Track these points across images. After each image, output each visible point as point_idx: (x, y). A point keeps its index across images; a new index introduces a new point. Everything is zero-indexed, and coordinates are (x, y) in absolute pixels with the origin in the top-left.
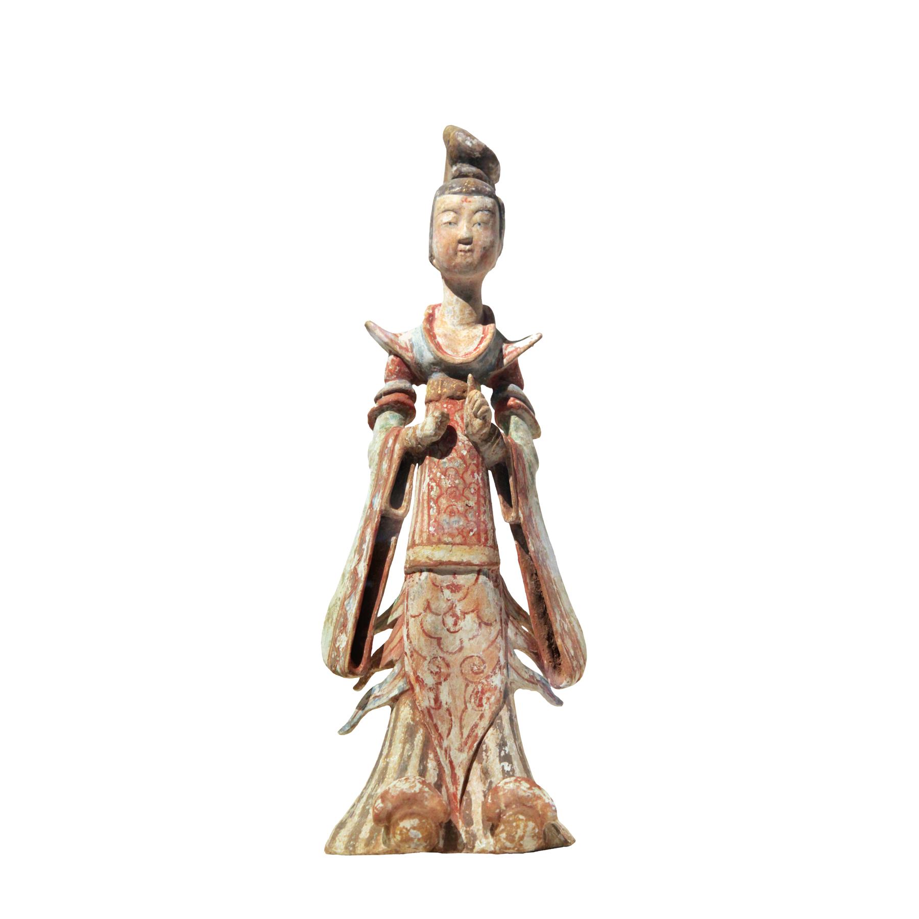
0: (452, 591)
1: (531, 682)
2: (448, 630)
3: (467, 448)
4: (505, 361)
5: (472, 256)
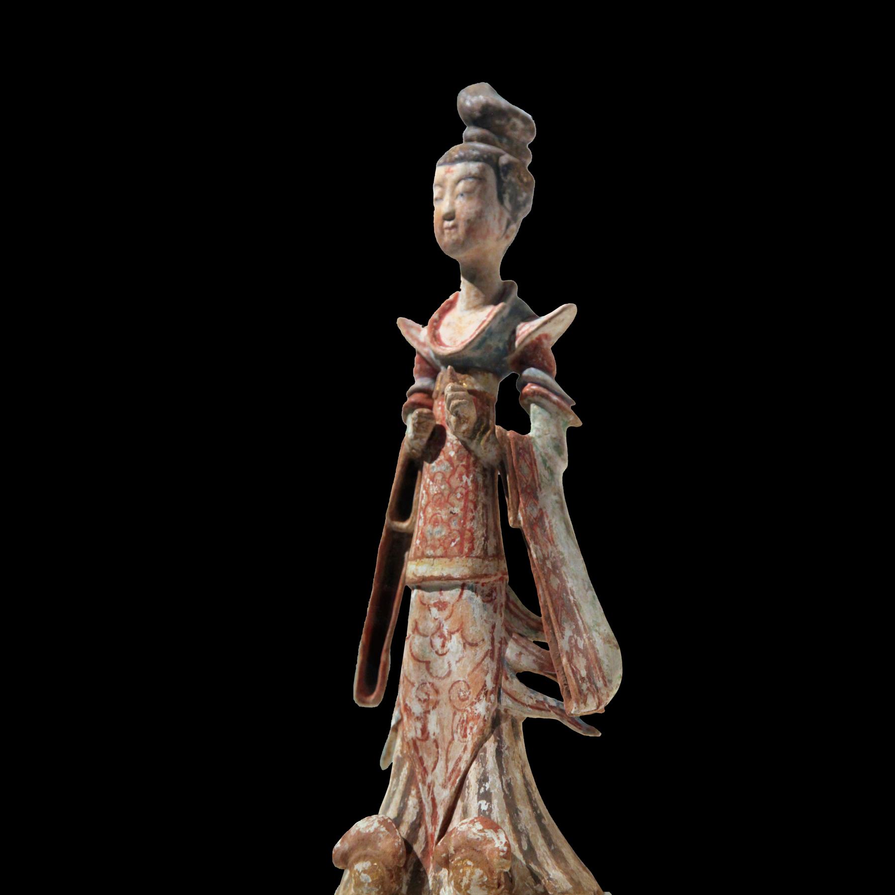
0: (439, 609)
2: (437, 652)
3: (456, 448)
4: (517, 343)
5: (457, 232)
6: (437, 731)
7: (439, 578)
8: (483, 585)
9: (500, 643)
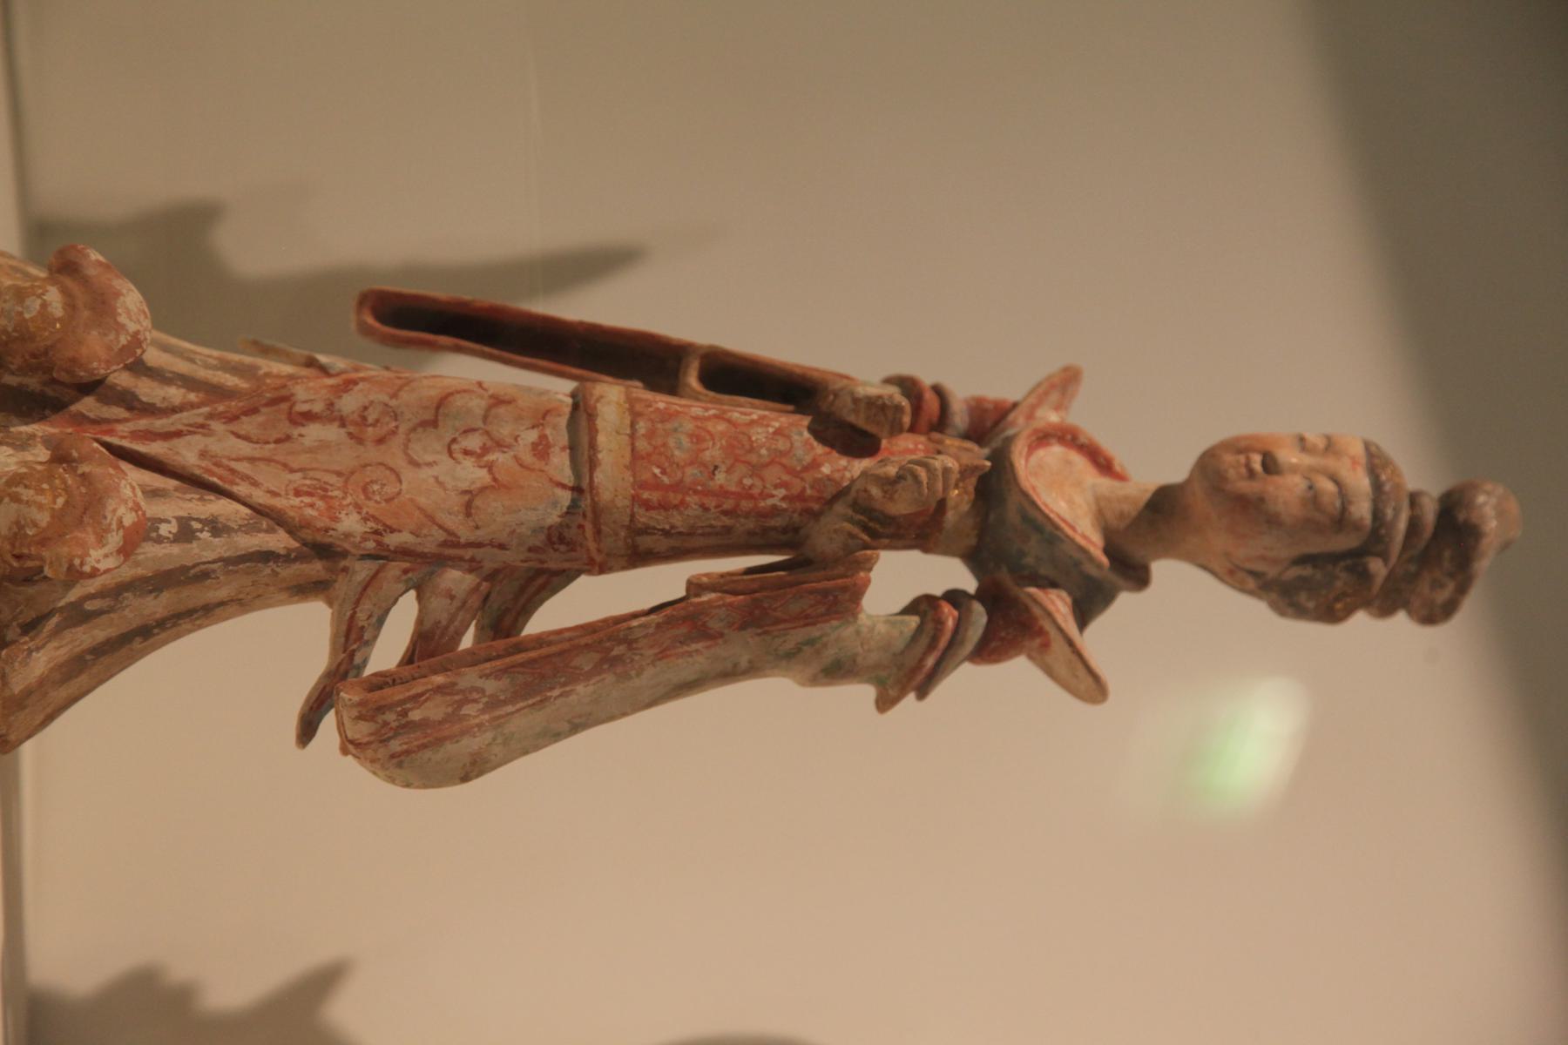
0: (535, 446)
1: (352, 638)
2: (454, 440)
3: (837, 476)
4: (1032, 590)
6: (307, 442)
7: (593, 445)
8: (581, 527)
9: (472, 560)
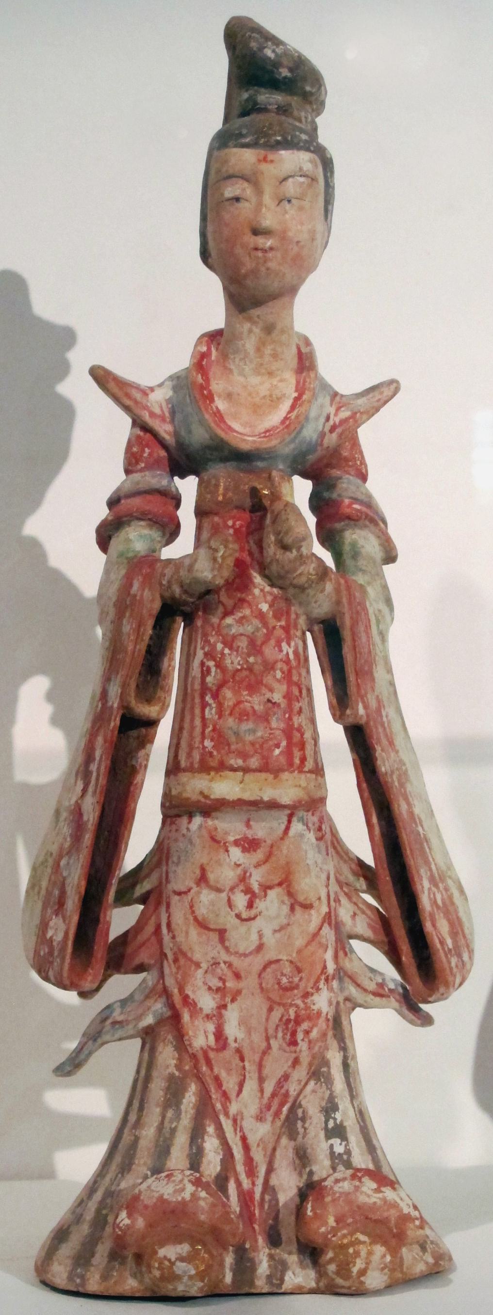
2: (238, 916)
3: (269, 598)
6: (241, 1035)
